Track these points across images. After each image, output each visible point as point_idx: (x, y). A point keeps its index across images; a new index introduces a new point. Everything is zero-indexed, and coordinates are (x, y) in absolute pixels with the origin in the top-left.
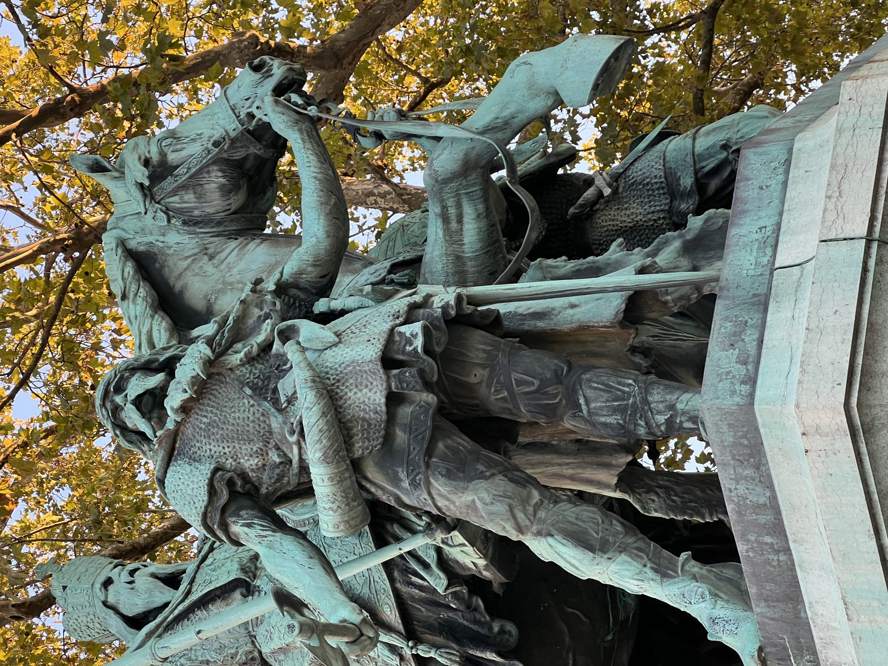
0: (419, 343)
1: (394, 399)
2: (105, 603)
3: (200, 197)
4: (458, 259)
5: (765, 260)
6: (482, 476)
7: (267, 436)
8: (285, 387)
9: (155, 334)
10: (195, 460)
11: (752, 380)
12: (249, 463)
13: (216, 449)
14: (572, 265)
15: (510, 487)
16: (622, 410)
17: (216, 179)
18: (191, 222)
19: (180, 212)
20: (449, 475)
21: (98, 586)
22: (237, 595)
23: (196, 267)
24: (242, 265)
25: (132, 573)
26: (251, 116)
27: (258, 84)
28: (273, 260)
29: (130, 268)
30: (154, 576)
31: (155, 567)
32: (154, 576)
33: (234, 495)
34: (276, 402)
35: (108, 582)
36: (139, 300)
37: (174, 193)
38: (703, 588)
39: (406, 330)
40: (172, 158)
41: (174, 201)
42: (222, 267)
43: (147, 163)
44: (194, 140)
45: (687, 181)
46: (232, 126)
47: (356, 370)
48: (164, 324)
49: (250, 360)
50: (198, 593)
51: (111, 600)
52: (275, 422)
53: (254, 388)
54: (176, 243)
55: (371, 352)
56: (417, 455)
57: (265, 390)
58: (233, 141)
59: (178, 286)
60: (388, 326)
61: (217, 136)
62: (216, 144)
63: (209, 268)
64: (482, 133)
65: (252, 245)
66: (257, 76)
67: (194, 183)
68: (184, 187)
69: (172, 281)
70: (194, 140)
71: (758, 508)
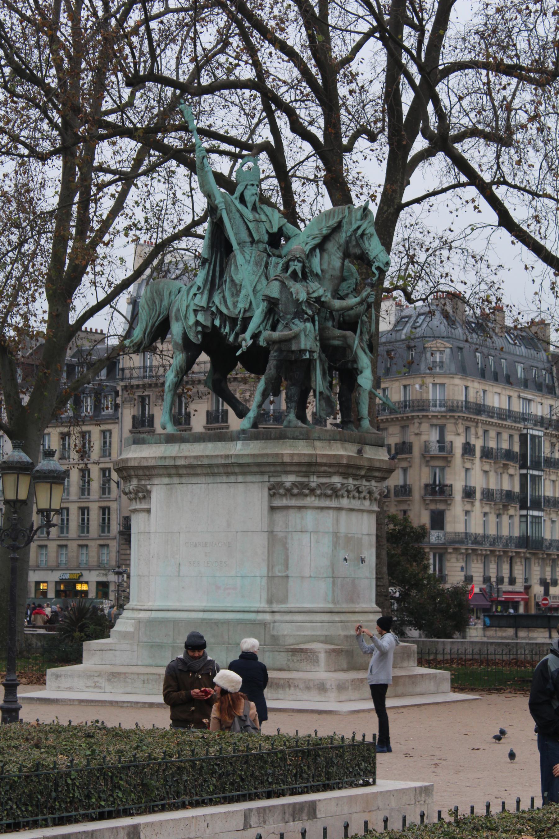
1: (293, 352)
4: (329, 339)
7: (286, 313)
8: (296, 321)
10: (281, 292)
11: (294, 438)
12: (280, 307)
13: (283, 300)
14: (326, 368)
17: (358, 251)
18: (348, 242)
19: (350, 239)
33: (273, 303)
34: (293, 318)
35: (253, 185)
39: (307, 354)
40: (365, 237)
41: (353, 238)
43: (364, 231)
45: (355, 366)
46: (372, 258)
47: (299, 343)
50: (251, 225)
51: (249, 187)
54: (343, 237)
55: (303, 347)
60: (308, 348)
63: (335, 248)
67: (358, 245)
68: (357, 241)
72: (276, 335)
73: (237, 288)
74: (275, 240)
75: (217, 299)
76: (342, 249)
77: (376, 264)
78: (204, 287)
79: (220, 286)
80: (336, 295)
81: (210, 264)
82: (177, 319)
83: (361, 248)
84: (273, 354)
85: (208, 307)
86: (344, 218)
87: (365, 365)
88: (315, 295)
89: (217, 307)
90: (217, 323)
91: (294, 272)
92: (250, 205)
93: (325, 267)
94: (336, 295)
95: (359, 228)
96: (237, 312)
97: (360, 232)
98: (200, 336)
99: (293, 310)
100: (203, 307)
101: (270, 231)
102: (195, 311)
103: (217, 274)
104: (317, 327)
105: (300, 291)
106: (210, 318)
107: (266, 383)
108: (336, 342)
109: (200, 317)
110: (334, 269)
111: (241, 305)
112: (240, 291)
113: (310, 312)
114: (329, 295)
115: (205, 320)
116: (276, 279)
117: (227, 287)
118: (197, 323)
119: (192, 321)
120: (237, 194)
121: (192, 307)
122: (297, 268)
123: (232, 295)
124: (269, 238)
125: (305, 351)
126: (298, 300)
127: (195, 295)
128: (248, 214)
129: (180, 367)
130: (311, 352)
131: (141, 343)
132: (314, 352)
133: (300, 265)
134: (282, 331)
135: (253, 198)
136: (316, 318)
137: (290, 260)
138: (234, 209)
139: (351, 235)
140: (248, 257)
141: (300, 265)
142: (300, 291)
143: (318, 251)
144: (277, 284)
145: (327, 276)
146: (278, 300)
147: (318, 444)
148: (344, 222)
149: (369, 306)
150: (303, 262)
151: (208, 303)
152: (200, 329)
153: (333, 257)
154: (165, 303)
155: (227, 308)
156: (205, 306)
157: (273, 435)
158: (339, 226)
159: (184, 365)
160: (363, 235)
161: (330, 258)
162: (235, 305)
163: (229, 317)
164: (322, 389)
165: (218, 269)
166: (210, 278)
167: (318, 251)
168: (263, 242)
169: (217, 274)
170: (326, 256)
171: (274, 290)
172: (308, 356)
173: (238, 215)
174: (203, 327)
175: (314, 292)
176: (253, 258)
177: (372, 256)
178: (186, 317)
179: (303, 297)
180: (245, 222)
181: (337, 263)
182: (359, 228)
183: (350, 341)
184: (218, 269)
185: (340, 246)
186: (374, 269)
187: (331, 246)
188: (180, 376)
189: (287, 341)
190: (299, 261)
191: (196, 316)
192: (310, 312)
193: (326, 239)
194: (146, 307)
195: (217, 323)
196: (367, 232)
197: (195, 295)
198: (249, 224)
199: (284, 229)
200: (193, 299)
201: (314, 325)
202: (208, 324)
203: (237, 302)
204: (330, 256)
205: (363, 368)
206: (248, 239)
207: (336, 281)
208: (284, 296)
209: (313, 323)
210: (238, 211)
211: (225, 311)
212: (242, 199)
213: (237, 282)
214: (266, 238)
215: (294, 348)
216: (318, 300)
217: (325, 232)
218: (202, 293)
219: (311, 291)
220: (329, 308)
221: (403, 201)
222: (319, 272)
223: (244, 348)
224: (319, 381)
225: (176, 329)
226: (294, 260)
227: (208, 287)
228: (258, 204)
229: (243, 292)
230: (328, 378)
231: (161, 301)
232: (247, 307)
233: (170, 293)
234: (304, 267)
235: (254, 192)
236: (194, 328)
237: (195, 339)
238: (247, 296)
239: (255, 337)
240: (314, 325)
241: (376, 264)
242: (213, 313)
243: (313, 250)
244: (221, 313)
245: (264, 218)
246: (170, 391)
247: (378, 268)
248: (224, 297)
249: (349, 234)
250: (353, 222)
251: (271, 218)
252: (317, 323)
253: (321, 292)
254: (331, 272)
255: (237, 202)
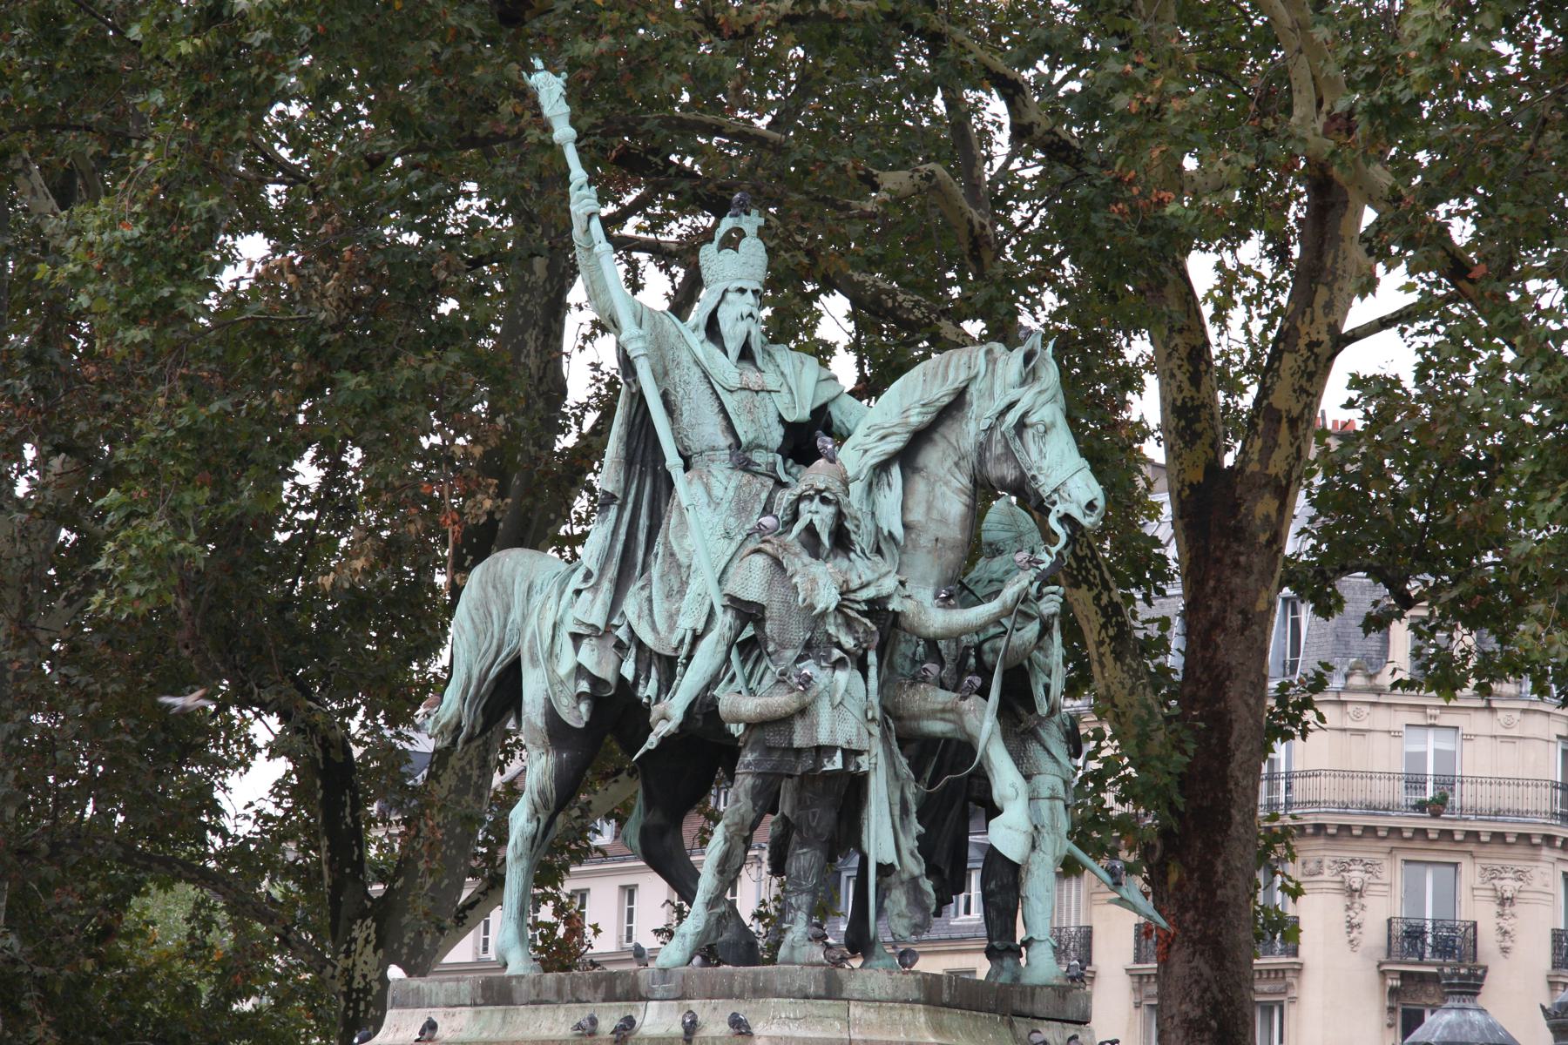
0: (829, 767)
1: (799, 751)
2: (726, 291)
3: (998, 458)
5: (856, 996)
6: (755, 804)
7: (783, 646)
9: (894, 438)
11: (790, 995)
12: (769, 627)
13: (774, 611)
15: (749, 822)
16: (798, 877)
17: (1010, 474)
18: (982, 448)
19: (989, 439)
20: (754, 787)
21: (739, 284)
22: (730, 440)
23: (951, 451)
24: (949, 493)
25: (751, 315)
26: (1054, 503)
27: (1079, 506)
28: (951, 520)
29: (946, 400)
30: (749, 334)
31: (756, 331)
32: (749, 334)
34: (800, 659)
35: (742, 291)
36: (920, 419)
37: (1003, 434)
38: (701, 926)
40: (1029, 434)
42: (949, 477)
43: (1025, 415)
44: (1041, 451)
46: (1045, 491)
47: (813, 727)
48: (900, 445)
49: (830, 635)
50: (730, 402)
51: (730, 296)
52: (790, 654)
53: (810, 639)
54: (969, 431)
55: (823, 738)
56: (767, 767)
57: (809, 649)
58: (1036, 493)
59: (937, 437)
60: (841, 742)
61: (1040, 477)
62: (1034, 477)
63: (949, 463)
64: (985, 749)
65: (965, 498)
66: (1084, 504)
67: (1009, 454)
68: (1007, 446)
69: (942, 430)
70: (1041, 451)
71: (731, 987)
72: (750, 706)
73: (680, 573)
74: (806, 439)
75: (631, 605)
76: (967, 466)
77: (1061, 508)
78: (602, 570)
79: (645, 567)
80: (959, 591)
81: (621, 508)
82: (534, 661)
83: (1018, 465)
84: (748, 757)
85: (610, 628)
86: (975, 377)
87: (1010, 792)
88: (869, 593)
89: (630, 626)
90: (628, 670)
91: (810, 529)
92: (733, 347)
93: (916, 515)
94: (959, 591)
95: (1011, 406)
96: (675, 643)
97: (1012, 418)
98: (583, 707)
99: (800, 635)
100: (598, 629)
101: (790, 418)
102: (577, 638)
103: (642, 537)
104: (873, 683)
105: (821, 583)
106: (611, 656)
107: (726, 840)
108: (937, 727)
109: (588, 656)
110: (943, 521)
111: (689, 621)
112: (687, 583)
113: (848, 642)
114: (925, 595)
115: (599, 663)
116: (758, 551)
117: (656, 570)
118: (580, 670)
119: (565, 666)
120: (698, 313)
121: (570, 626)
122: (817, 520)
123: (669, 596)
124: (785, 437)
125: (829, 750)
126: (812, 607)
127: (578, 592)
128: (725, 368)
129: (542, 793)
130: (850, 754)
131: (458, 727)
132: (859, 753)
133: (829, 511)
134: (770, 695)
135: (743, 327)
136: (872, 658)
137: (800, 498)
138: (685, 358)
139: (991, 428)
140: (718, 491)
141: (829, 511)
142: (821, 583)
143: (896, 471)
144: (760, 561)
145: (925, 541)
146: (761, 608)
147: (856, 1011)
148: (973, 389)
149: (1045, 630)
150: (838, 503)
151: (610, 616)
152: (584, 686)
153: (940, 489)
154: (515, 615)
155: (654, 628)
156: (601, 624)
157: (736, 990)
158: (957, 404)
159: (550, 786)
160: (1021, 426)
161: (932, 491)
162: (672, 618)
163: (659, 656)
164: (889, 857)
165: (643, 521)
166: (619, 547)
167: (896, 471)
168: (766, 449)
169: (642, 537)
170: (920, 485)
171: (752, 582)
172: (837, 763)
173: (696, 374)
174: (595, 682)
175: (863, 586)
176: (731, 493)
177: (1046, 486)
178: (552, 654)
179: (827, 598)
180: (715, 392)
181: (954, 505)
182: (1011, 406)
183: (971, 722)
184: (643, 521)
185: (963, 458)
186: (1053, 522)
187: (934, 458)
188: (543, 818)
189: (783, 722)
190: (824, 501)
191: (577, 649)
192: (848, 642)
193: (920, 438)
194: (468, 625)
195: (628, 670)
196: (1032, 419)
197: (578, 592)
198: (725, 397)
199: (834, 411)
200: (571, 604)
201: (865, 677)
202: (607, 673)
203: (678, 611)
204: (931, 485)
205: (1002, 797)
206: (723, 441)
207: (951, 556)
208: (777, 598)
209: (863, 668)
210: (697, 363)
211: (648, 639)
212: (712, 329)
213: (682, 558)
214: (776, 436)
215: (799, 741)
216: (876, 608)
217: (916, 419)
218: (595, 588)
219: (855, 584)
220: (913, 631)
221: (1346, 329)
222: (899, 532)
223: (652, 742)
224: (883, 835)
225: (534, 686)
226: (811, 498)
227: (612, 571)
228: (756, 346)
229: (694, 587)
230: (916, 828)
231: (508, 610)
232: (700, 627)
233: (530, 587)
234: (840, 516)
235: (746, 312)
236: (571, 684)
237: (577, 715)
238: (702, 595)
239: (704, 710)
240: (865, 677)
241: (1061, 508)
242: (619, 645)
243: (882, 468)
244: (640, 645)
245: (771, 380)
246: (519, 858)
247: (1066, 519)
248: (650, 600)
249: (985, 424)
250: (998, 390)
251: (792, 381)
252: (873, 672)
253: (889, 584)
254: (934, 530)
255: (696, 340)
